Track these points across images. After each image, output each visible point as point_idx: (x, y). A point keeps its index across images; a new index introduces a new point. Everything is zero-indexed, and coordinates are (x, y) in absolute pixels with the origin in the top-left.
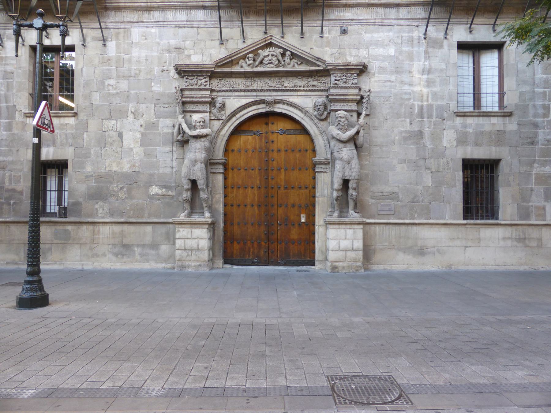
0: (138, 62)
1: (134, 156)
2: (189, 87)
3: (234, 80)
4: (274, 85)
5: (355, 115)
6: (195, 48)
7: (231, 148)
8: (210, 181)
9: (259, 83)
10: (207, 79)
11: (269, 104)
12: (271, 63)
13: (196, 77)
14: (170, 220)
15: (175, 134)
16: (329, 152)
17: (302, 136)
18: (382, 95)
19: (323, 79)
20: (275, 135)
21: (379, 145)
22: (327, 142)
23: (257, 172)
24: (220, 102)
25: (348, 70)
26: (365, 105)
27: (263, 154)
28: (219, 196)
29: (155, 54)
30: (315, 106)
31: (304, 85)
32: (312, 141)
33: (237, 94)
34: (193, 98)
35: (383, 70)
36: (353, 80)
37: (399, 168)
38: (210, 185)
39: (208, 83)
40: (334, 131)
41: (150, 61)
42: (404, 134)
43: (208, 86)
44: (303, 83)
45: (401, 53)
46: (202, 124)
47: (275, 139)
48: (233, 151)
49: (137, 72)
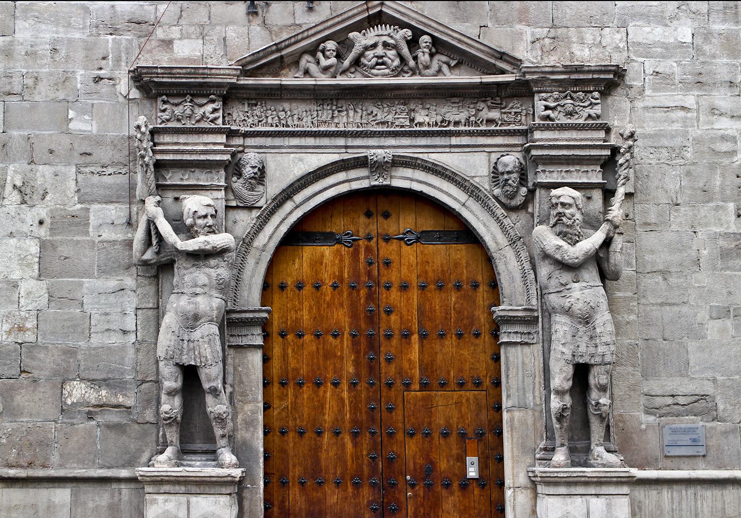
0: (31, 54)
1: (22, 301)
2: (170, 125)
3: (287, 106)
4: (390, 118)
5: (597, 195)
6: (182, 22)
7: (276, 282)
8: (230, 369)
9: (351, 113)
10: (218, 105)
11: (378, 167)
12: (383, 64)
13: (188, 98)
14: (124, 473)
15: (137, 245)
16: (533, 291)
17: (463, 247)
18: (666, 142)
19: (515, 106)
20: (394, 246)
21: (661, 272)
22: (527, 266)
23: (347, 341)
24: (253, 163)
25: (577, 82)
26: (622, 172)
27: (363, 293)
28: (254, 407)
29: (77, 35)
30: (496, 174)
31: (468, 120)
32: (489, 260)
33: (295, 141)
34: (183, 152)
35: (662, 79)
36: (590, 108)
37: (713, 330)
38: (230, 379)
39: (220, 113)
40: (547, 237)
41: (63, 53)
42: (721, 242)
43: (220, 121)
44: (462, 116)
45: (708, 36)
46: (210, 221)
47: (394, 257)
48: (283, 287)
49: (30, 82)
